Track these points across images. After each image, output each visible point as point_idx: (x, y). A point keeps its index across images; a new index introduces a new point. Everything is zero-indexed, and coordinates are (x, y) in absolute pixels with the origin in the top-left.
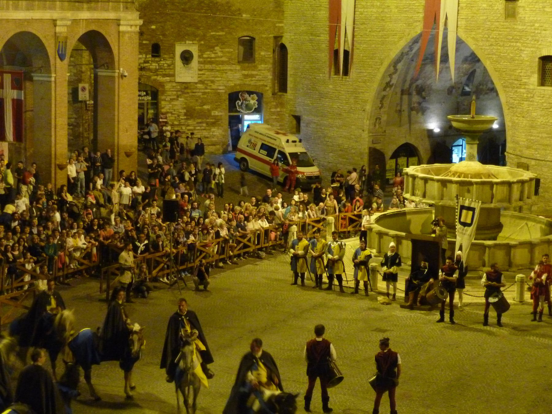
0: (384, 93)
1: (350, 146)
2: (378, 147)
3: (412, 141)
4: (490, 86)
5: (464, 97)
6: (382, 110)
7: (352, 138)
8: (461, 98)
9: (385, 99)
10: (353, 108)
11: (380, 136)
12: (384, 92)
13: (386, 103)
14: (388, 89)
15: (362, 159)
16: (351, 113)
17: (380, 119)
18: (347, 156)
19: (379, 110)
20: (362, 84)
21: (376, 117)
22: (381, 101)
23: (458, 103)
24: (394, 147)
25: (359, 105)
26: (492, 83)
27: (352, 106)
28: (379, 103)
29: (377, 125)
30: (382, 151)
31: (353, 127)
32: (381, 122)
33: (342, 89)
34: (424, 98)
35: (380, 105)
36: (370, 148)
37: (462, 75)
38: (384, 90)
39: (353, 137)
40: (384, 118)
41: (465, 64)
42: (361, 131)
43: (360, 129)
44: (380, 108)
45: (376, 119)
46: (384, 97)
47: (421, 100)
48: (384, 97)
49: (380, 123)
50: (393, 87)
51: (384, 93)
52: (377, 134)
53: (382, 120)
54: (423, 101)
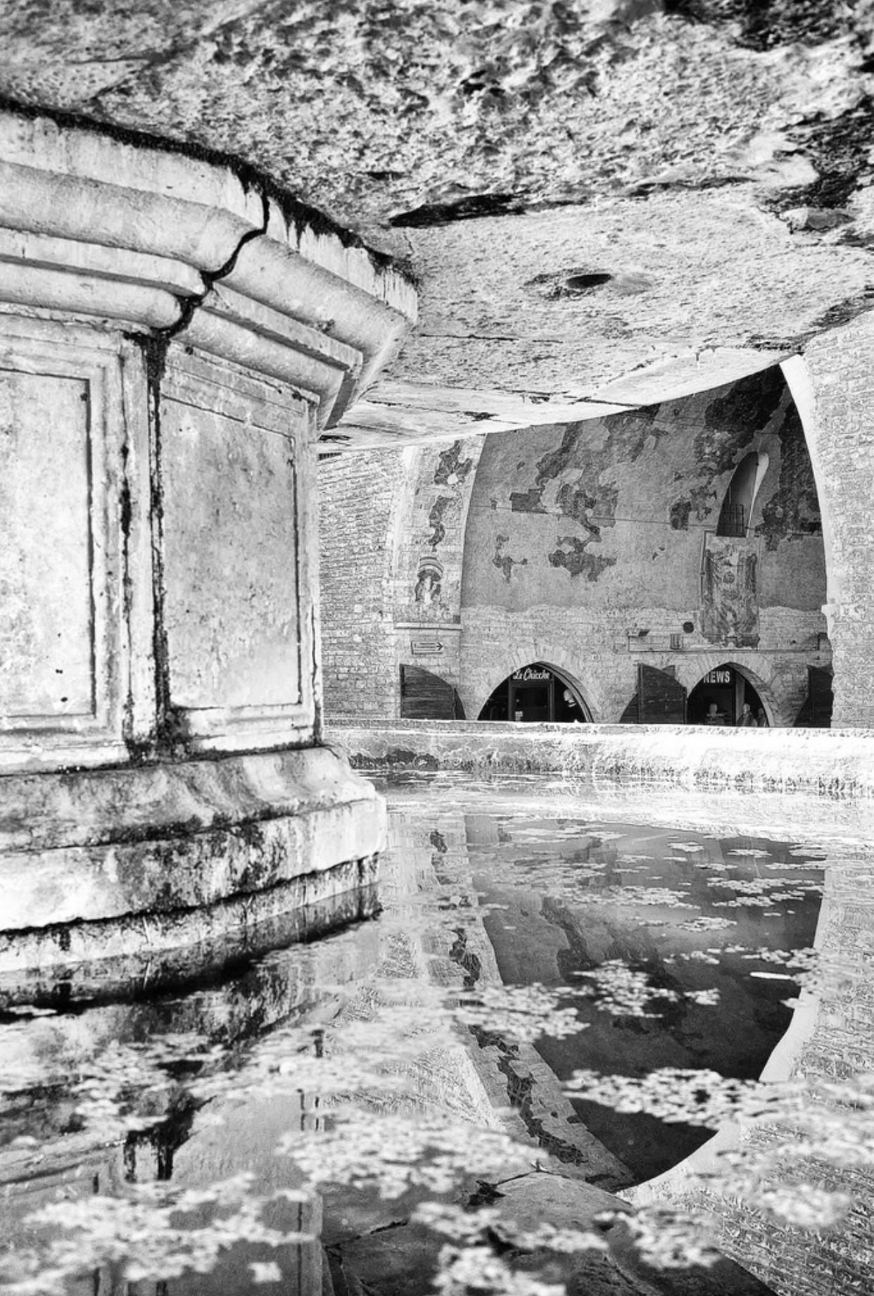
0: (439, 491)
1: (352, 670)
2: (435, 665)
3: (559, 658)
4: (805, 513)
5: (727, 540)
6: (438, 547)
7: (358, 644)
8: (716, 540)
9: (449, 512)
10: (356, 550)
11: (441, 633)
12: (441, 486)
13: (455, 521)
14: (453, 479)
15: (381, 705)
16: (349, 566)
17: (436, 577)
18: (345, 704)
19: (431, 548)
20: (376, 467)
21: (417, 572)
22: (432, 517)
23: (709, 556)
24: (498, 676)
25: (369, 535)
26: (815, 506)
27: (353, 543)
28: (428, 522)
29: (427, 596)
30: (450, 681)
31: (358, 608)
32: (439, 586)
33: (329, 498)
34: (594, 530)
35: (433, 531)
36: (402, 668)
37: (713, 465)
38: (440, 478)
39: (357, 639)
40: (452, 574)
41: (717, 427)
42: (375, 616)
43: (374, 609)
44: (435, 541)
45: (422, 576)
46: (441, 505)
47: (582, 534)
48: (441, 505)
49: (437, 591)
50: (473, 472)
51: (439, 491)
52: (426, 625)
53: (442, 582)
54: (590, 540)
